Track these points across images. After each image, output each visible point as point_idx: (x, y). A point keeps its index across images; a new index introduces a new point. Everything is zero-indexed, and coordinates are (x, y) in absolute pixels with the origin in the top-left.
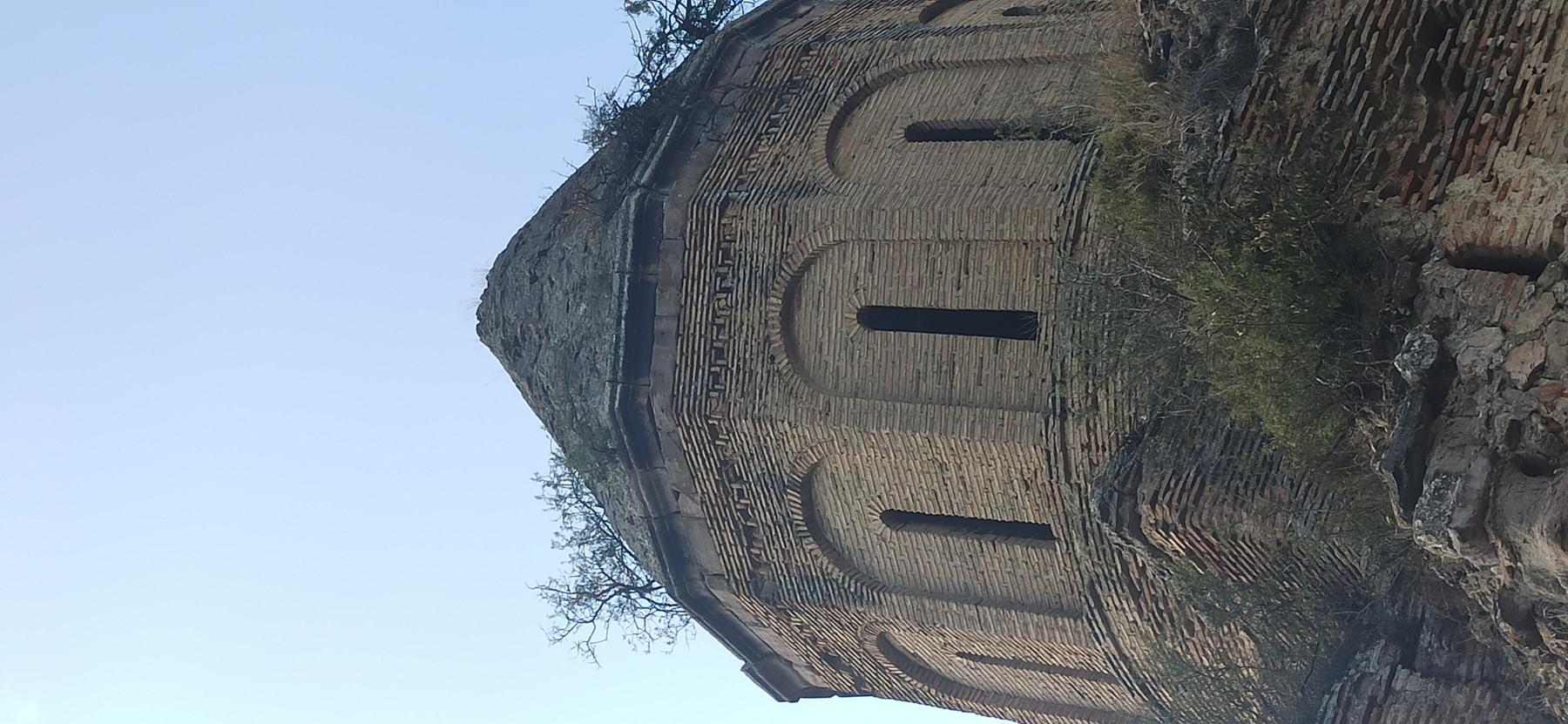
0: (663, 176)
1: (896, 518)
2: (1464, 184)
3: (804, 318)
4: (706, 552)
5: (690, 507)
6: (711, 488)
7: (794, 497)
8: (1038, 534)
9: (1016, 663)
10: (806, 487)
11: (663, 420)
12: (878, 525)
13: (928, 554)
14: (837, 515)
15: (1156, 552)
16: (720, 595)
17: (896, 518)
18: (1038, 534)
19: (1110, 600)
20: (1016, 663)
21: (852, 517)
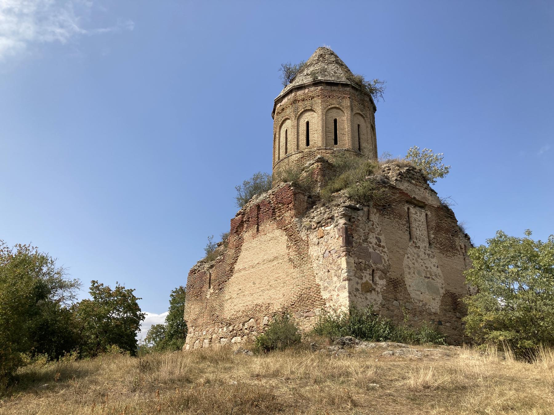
0: (353, 87)
1: (308, 123)
2: (375, 210)
3: (335, 110)
4: (300, 93)
5: (307, 91)
6: (310, 95)
7: (310, 108)
8: (308, 144)
9: (286, 138)
10: (311, 110)
11: (320, 88)
12: (306, 120)
13: (303, 128)
14: (307, 114)
15: (313, 164)
16: (293, 94)
17: (308, 123)
18: (308, 144)
19: (301, 154)
20: (286, 138)
21: (307, 117)
